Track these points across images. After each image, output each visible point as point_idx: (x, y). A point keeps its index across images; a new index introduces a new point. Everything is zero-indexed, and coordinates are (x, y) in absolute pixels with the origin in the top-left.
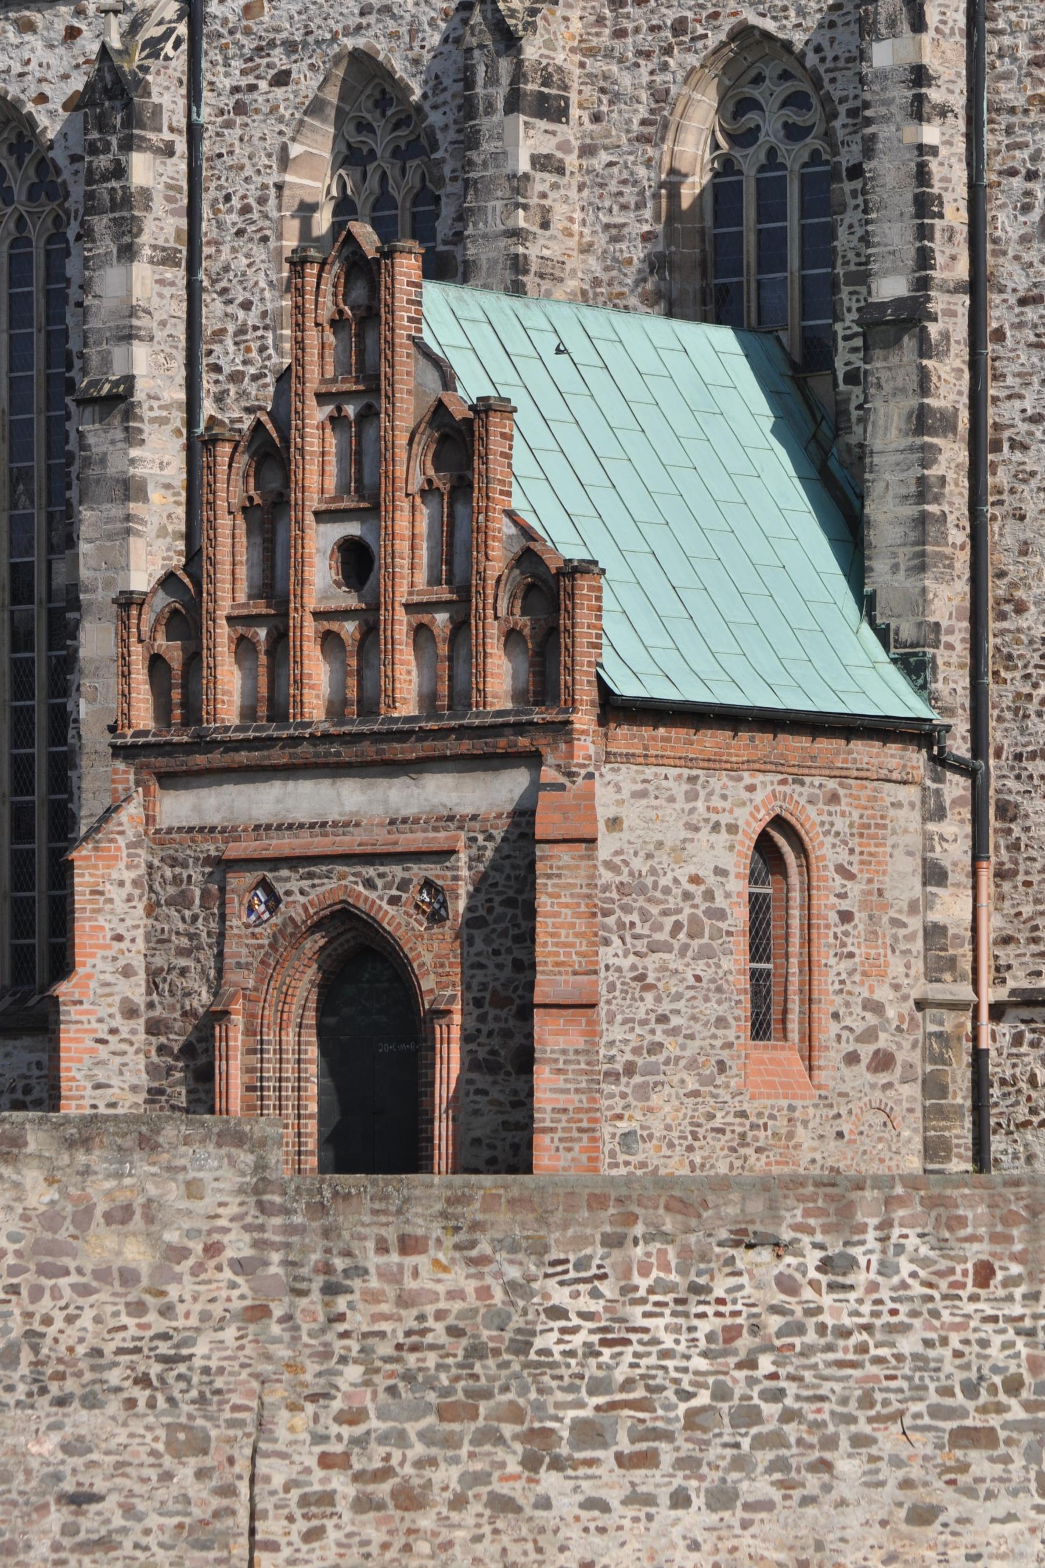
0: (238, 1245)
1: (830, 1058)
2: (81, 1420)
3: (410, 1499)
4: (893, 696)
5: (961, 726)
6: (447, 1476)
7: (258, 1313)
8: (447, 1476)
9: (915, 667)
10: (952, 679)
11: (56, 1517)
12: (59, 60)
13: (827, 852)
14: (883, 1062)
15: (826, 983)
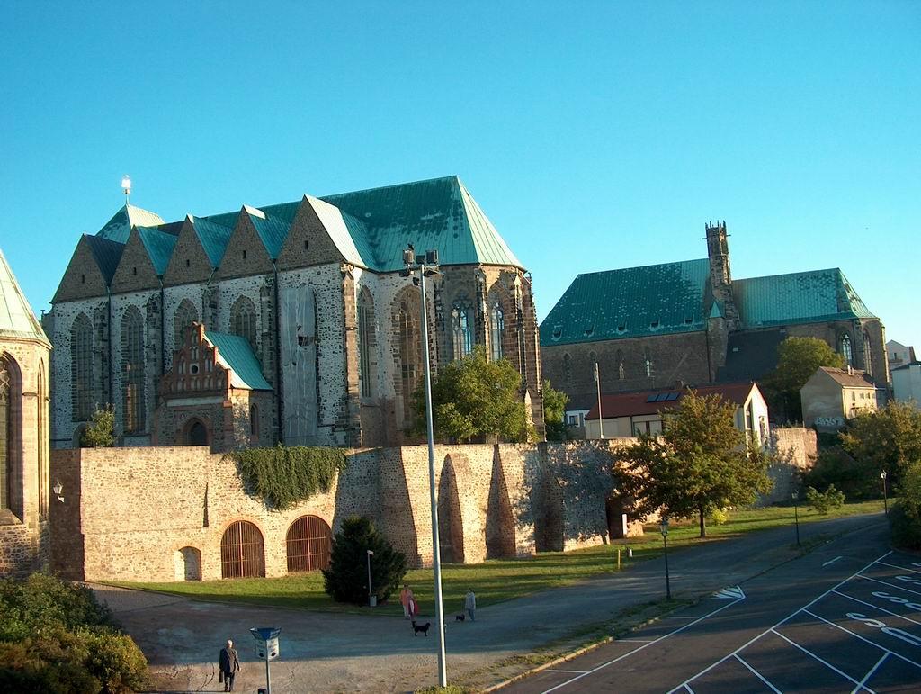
0: (204, 464)
1: (261, 437)
2: (183, 490)
3: (228, 499)
4: (266, 386)
5: (276, 390)
6: (233, 496)
7: (207, 474)
8: (233, 496)
9: (270, 383)
10: (275, 385)
11: (180, 503)
12: (143, 300)
13: (260, 408)
14: (268, 437)
15: (260, 426)
